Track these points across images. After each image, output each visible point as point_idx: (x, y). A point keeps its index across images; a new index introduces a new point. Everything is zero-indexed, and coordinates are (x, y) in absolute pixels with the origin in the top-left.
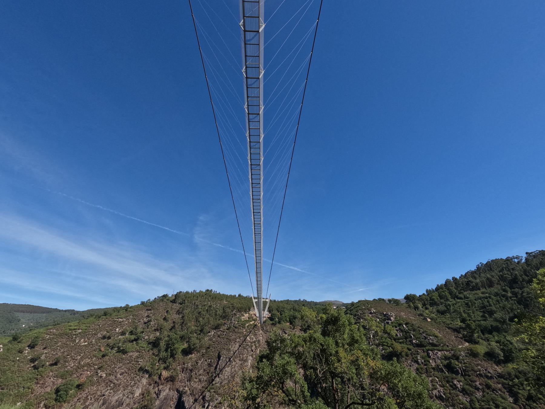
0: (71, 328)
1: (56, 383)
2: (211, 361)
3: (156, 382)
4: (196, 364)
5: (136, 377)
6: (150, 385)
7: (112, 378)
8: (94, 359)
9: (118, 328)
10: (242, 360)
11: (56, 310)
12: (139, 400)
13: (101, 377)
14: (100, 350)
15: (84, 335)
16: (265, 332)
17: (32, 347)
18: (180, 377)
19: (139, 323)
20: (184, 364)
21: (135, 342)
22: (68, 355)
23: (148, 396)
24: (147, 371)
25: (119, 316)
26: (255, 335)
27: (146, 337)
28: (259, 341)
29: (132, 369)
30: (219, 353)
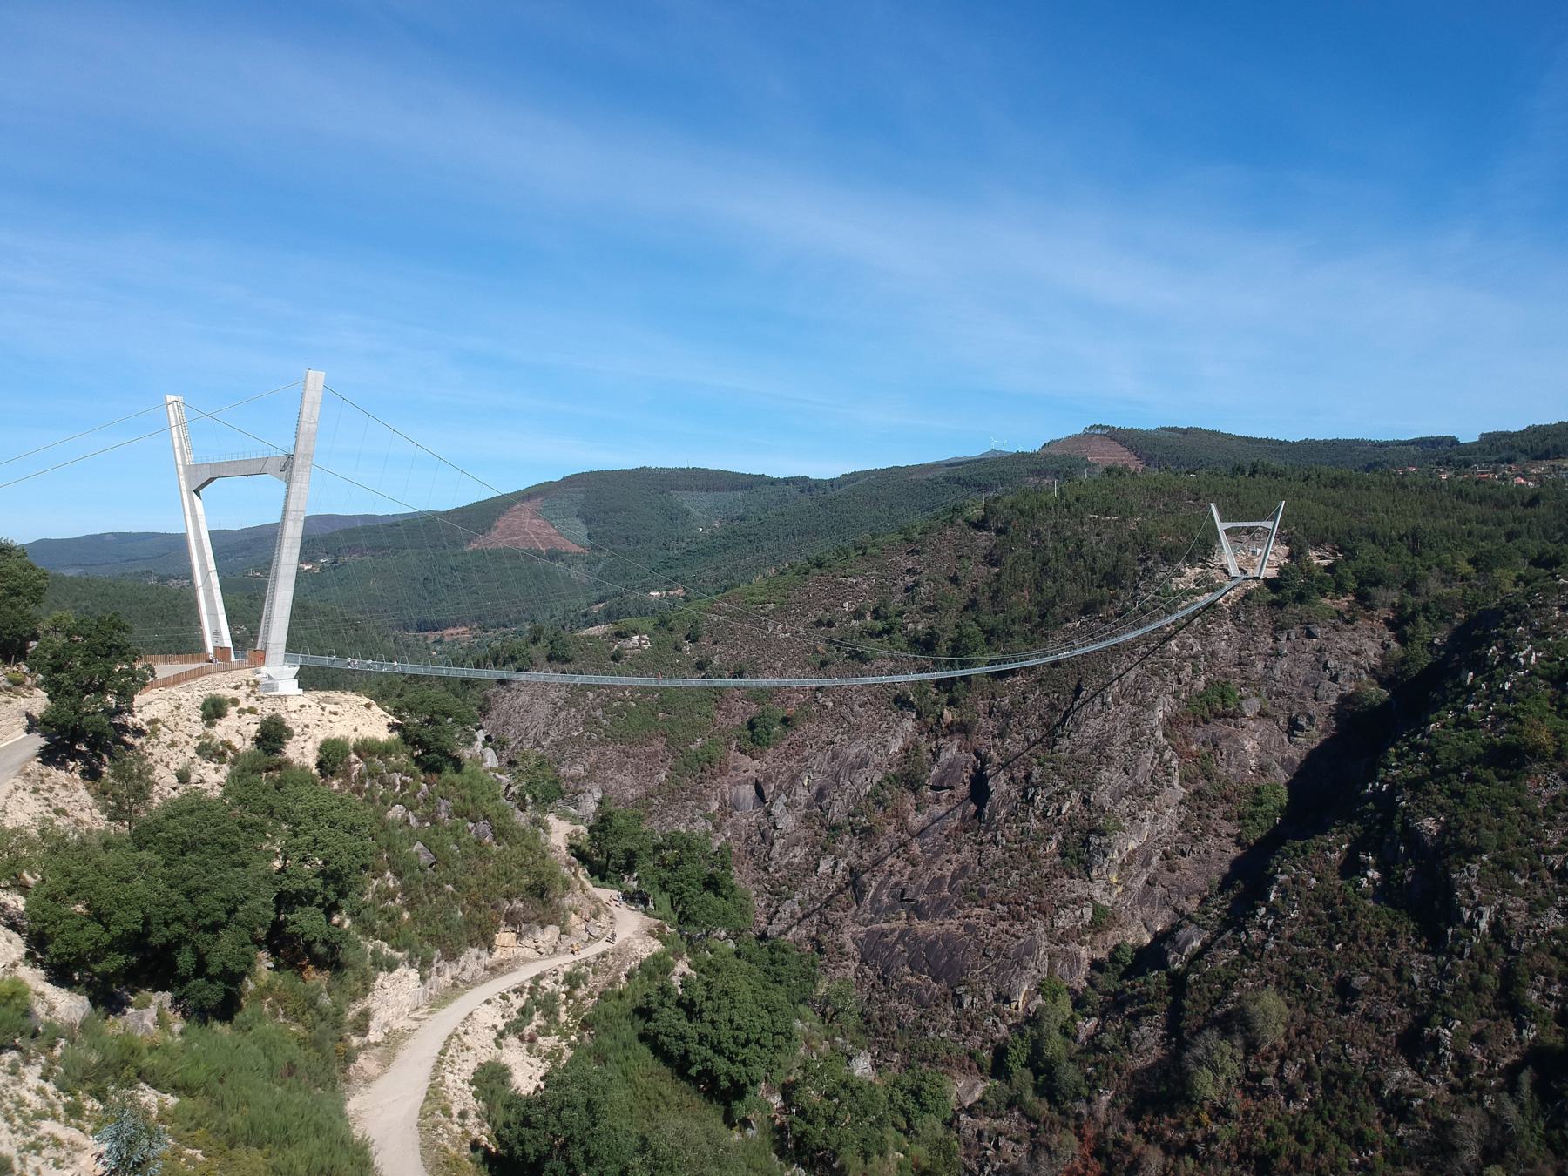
0: (753, 598)
1: (748, 710)
2: (1058, 699)
3: (932, 730)
4: (1022, 701)
5: (890, 715)
6: (920, 734)
7: (845, 710)
8: (808, 668)
9: (847, 600)
10: (1140, 704)
11: (762, 480)
12: (900, 759)
13: (825, 707)
14: (818, 652)
15: (781, 614)
17: (693, 638)
18: (984, 725)
19: (893, 589)
20: (994, 698)
21: (886, 637)
22: (758, 659)
23: (916, 755)
24: (911, 706)
26: (1204, 636)
27: (910, 627)
28: (1213, 654)
29: (883, 698)
30: (1081, 680)
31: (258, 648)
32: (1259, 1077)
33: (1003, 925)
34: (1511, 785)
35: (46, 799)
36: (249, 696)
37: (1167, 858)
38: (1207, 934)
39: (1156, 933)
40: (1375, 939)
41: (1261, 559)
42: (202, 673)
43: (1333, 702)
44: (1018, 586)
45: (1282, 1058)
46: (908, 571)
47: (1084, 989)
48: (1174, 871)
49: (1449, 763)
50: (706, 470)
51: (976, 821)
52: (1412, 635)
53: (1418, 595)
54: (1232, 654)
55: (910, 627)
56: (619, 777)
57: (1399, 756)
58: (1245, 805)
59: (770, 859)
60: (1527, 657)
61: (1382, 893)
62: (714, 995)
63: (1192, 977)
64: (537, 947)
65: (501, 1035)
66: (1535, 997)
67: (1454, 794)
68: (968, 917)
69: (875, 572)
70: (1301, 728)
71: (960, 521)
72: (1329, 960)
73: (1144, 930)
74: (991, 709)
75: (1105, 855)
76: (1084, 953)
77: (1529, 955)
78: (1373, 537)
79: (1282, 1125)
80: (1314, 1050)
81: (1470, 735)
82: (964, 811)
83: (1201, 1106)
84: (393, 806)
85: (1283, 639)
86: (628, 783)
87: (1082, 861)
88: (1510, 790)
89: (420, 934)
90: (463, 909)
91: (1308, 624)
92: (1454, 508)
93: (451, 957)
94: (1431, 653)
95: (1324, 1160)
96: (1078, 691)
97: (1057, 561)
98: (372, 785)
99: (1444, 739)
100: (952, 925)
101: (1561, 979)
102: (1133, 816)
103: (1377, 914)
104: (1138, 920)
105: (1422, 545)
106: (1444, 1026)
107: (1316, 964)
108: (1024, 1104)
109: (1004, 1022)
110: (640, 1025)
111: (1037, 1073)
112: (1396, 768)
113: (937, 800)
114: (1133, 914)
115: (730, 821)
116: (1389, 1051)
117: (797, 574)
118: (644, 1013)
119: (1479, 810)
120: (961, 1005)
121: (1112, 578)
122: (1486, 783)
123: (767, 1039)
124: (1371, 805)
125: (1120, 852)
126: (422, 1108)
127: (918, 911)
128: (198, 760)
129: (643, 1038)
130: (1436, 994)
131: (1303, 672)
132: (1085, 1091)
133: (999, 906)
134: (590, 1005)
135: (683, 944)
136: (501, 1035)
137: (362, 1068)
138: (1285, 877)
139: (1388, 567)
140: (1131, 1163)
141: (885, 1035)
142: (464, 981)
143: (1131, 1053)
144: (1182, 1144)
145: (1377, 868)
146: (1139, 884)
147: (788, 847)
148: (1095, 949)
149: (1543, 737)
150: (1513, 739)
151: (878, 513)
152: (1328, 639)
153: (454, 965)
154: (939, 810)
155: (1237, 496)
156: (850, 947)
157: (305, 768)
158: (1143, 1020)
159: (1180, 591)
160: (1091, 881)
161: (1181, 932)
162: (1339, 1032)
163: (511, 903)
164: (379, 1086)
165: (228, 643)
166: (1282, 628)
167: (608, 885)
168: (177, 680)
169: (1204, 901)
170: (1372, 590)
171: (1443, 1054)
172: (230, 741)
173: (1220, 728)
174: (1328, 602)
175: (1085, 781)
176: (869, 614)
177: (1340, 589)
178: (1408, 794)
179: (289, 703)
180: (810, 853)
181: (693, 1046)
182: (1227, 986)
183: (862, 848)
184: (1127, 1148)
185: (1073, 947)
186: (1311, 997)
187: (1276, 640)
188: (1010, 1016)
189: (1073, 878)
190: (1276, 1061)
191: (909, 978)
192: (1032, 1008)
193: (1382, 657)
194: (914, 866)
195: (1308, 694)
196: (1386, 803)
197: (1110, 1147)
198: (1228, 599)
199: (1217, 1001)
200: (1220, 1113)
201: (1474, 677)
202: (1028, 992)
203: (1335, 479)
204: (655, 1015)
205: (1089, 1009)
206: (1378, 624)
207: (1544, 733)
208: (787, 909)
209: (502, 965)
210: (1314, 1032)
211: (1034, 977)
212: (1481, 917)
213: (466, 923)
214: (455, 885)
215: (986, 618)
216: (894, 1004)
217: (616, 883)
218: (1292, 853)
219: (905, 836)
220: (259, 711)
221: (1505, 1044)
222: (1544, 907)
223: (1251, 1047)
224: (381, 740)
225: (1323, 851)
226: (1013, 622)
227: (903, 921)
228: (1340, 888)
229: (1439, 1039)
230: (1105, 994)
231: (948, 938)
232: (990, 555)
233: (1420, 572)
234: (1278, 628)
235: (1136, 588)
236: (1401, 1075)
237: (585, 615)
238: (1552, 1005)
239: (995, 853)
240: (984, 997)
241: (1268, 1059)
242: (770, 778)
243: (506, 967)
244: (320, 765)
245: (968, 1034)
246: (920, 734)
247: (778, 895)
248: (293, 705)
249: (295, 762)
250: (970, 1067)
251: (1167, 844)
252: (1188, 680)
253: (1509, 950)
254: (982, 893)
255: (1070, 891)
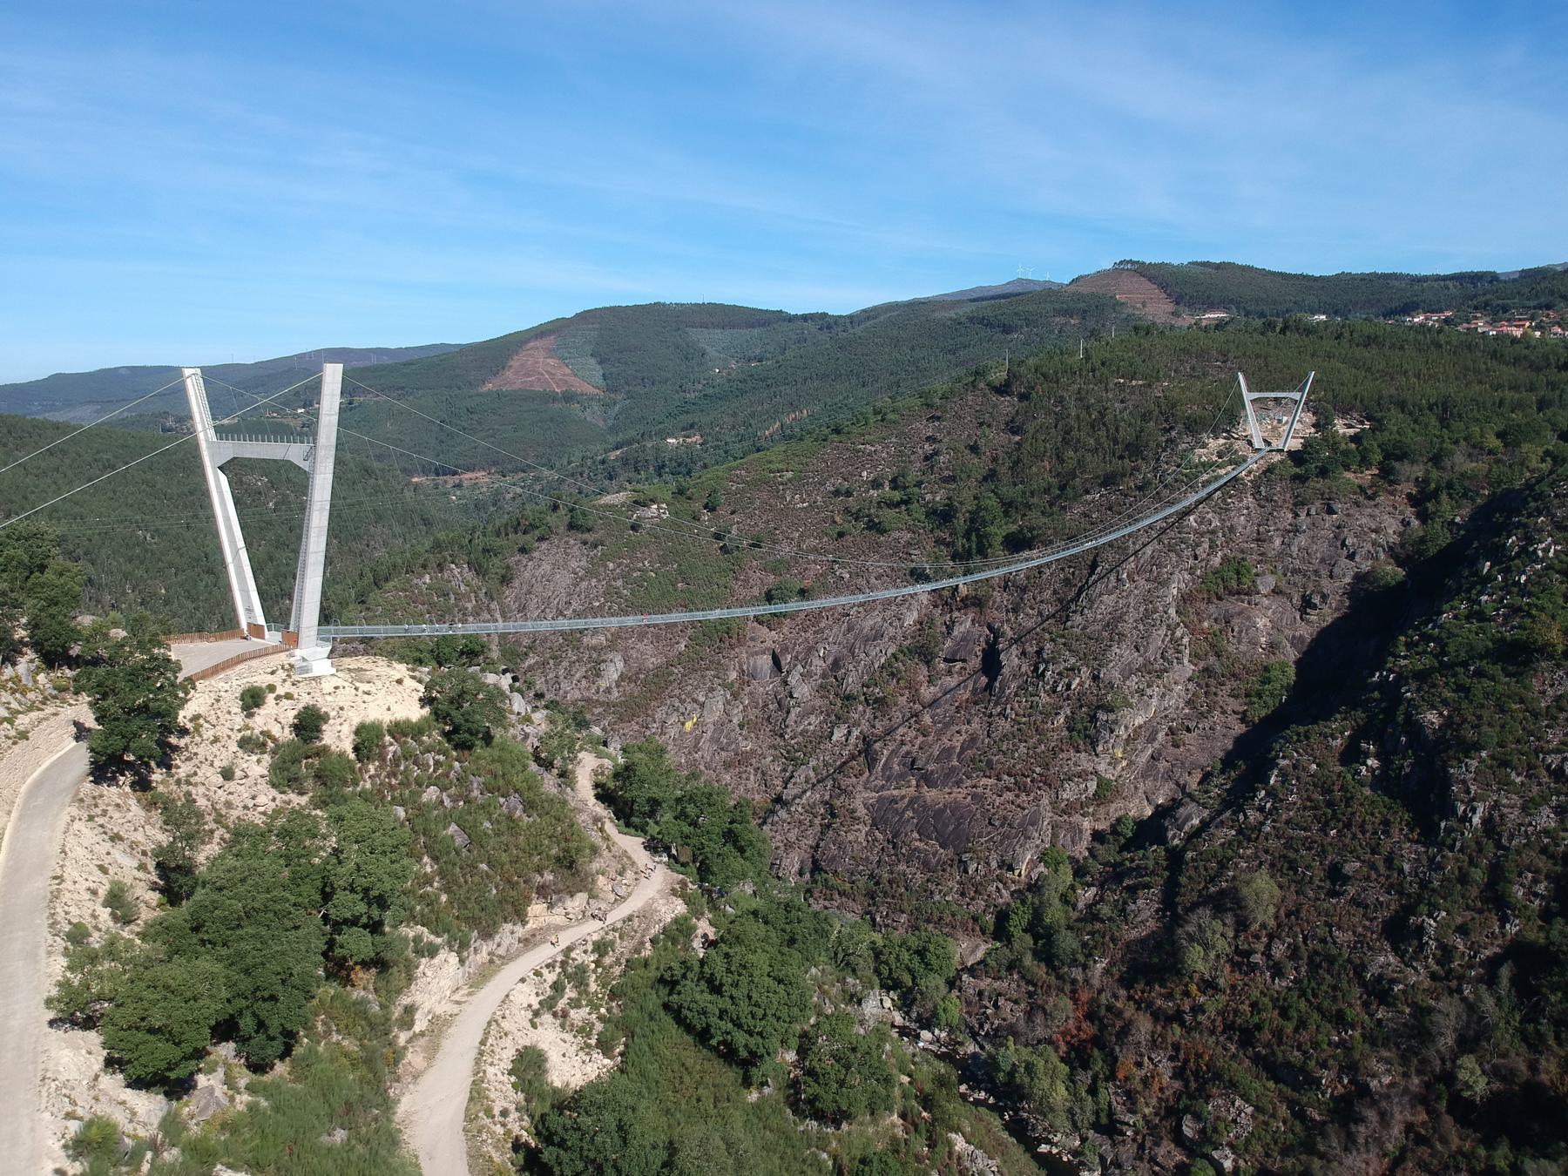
2: (1073, 573)
3: (946, 603)
6: (936, 606)
8: (825, 539)
10: (1155, 580)
15: (798, 483)
16: (1263, 503)
18: (998, 599)
19: (912, 458)
21: (903, 507)
25: (867, 437)
26: (1223, 510)
27: (928, 497)
28: (1232, 529)
30: (1097, 555)
31: (291, 629)
32: (1248, 954)
33: (1009, 796)
34: (1517, 682)
35: (102, 826)
36: (284, 681)
37: (1173, 734)
38: (1206, 813)
39: (1158, 806)
40: (1369, 827)
41: (1286, 427)
42: (240, 659)
43: (1348, 580)
44: (1039, 457)
45: (1271, 937)
46: (928, 439)
47: (1085, 858)
48: (1178, 747)
49: (1457, 656)
50: (722, 306)
51: (987, 694)
52: (1434, 513)
53: (1443, 468)
54: (1251, 530)
55: (928, 497)
56: (640, 646)
57: (1409, 645)
58: (1253, 682)
59: (786, 727)
60: (1546, 551)
61: (1381, 782)
62: (733, 969)
63: (1190, 855)
64: (567, 914)
65: (536, 1014)
66: (1520, 893)
67: (1460, 688)
68: (975, 786)
69: (894, 440)
70: (1315, 607)
71: (982, 385)
72: (1323, 846)
73: (1146, 803)
74: (1006, 583)
75: (1112, 731)
76: (1087, 824)
77: (1518, 853)
78: (1402, 406)
79: (1266, 1000)
80: (1302, 931)
81: (1481, 628)
82: (975, 683)
83: (1191, 978)
84: (427, 787)
85: (1303, 516)
86: (649, 653)
87: (1089, 736)
88: (1515, 688)
89: (458, 918)
90: (496, 887)
91: (1330, 499)
92: (1487, 369)
93: (487, 935)
94: (1451, 531)
95: (1304, 1036)
96: (1093, 567)
97: (1079, 430)
98: (406, 767)
99: (1456, 631)
100: (960, 794)
101: (1548, 877)
102: (1141, 693)
103: (1373, 802)
104: (1140, 792)
105: (1452, 414)
106: (1430, 916)
107: (1310, 849)
108: (1024, 967)
109: (1006, 888)
110: (664, 991)
111: (1036, 938)
112: (1405, 658)
113: (950, 673)
114: (1136, 788)
115: (747, 689)
116: (1375, 936)
117: (816, 440)
118: (669, 983)
119: (1482, 706)
120: (966, 871)
121: (1134, 449)
122: (1493, 678)
123: (784, 1013)
124: (1376, 694)
125: (1126, 728)
126: (467, 1109)
127: (927, 779)
128: (240, 753)
129: (666, 1007)
130: (1424, 884)
131: (1321, 549)
132: (1081, 958)
133: (1006, 777)
134: (618, 973)
135: (704, 900)
136: (536, 1014)
137: (410, 1063)
138: (1286, 762)
139: (1414, 439)
140: (1122, 1028)
141: (893, 897)
142: (500, 957)
143: (1127, 924)
144: (1170, 1012)
145: (1377, 756)
146: (1143, 759)
147: (803, 716)
148: (1098, 820)
149: (1554, 636)
150: (1523, 635)
151: (898, 356)
152: (1348, 515)
153: (491, 943)
154: (951, 682)
155: (1266, 358)
156: (861, 812)
157: (342, 755)
158: (1140, 893)
159: (1203, 465)
160: (1097, 755)
161: (1181, 810)
162: (1327, 915)
163: (542, 876)
164: (427, 1081)
165: (261, 621)
166: (1303, 504)
167: (633, 831)
168: (215, 671)
169: (1206, 778)
170: (1397, 465)
171: (1427, 943)
172: (269, 731)
173: (1232, 605)
174: (1349, 475)
175: (1097, 659)
176: (887, 483)
177: (1365, 462)
178: (1414, 686)
179: (323, 685)
180: (825, 721)
181: (714, 1020)
182: (1223, 865)
183: (875, 718)
184: (1119, 1014)
185: (1076, 818)
186: (1303, 879)
187: (1296, 515)
188: (1013, 882)
189: (1078, 751)
190: (1265, 940)
191: (917, 844)
192: (1034, 876)
193: (1401, 534)
194: (924, 736)
195: (1324, 572)
196: (1391, 692)
197: (1103, 1012)
198: (1250, 472)
199: (1212, 880)
200: (1209, 986)
201: (1491, 567)
202: (1031, 860)
203: (1369, 337)
204: (678, 988)
205: (1089, 878)
206: (1400, 499)
207: (1555, 632)
208: (801, 774)
209: (534, 935)
210: (1303, 914)
211: (1037, 846)
212: (1474, 813)
213: (500, 902)
214: (489, 864)
215: (1004, 489)
216: (902, 867)
217: (641, 829)
218: (1295, 738)
219: (918, 707)
220: (296, 696)
221: (1487, 937)
222: (1537, 806)
223: (1242, 925)
224: (414, 719)
225: (1326, 737)
226: (1032, 493)
227: (912, 789)
228: (1339, 775)
229: (1424, 929)
230: (1105, 864)
231: (955, 807)
232: (1012, 421)
233: (1448, 445)
234: (1299, 503)
235: (1158, 459)
236: (1384, 960)
237: (603, 462)
238: (1537, 902)
239: (1004, 726)
240: (988, 864)
241: (1257, 937)
242: (787, 649)
243: (538, 937)
244: (356, 749)
245: (973, 899)
246: (936, 606)
247: (793, 760)
248: (327, 686)
249: (333, 748)
250: (973, 930)
251: (1173, 720)
252: (1204, 556)
253: (1499, 846)
254: (989, 764)
255: (1076, 764)
